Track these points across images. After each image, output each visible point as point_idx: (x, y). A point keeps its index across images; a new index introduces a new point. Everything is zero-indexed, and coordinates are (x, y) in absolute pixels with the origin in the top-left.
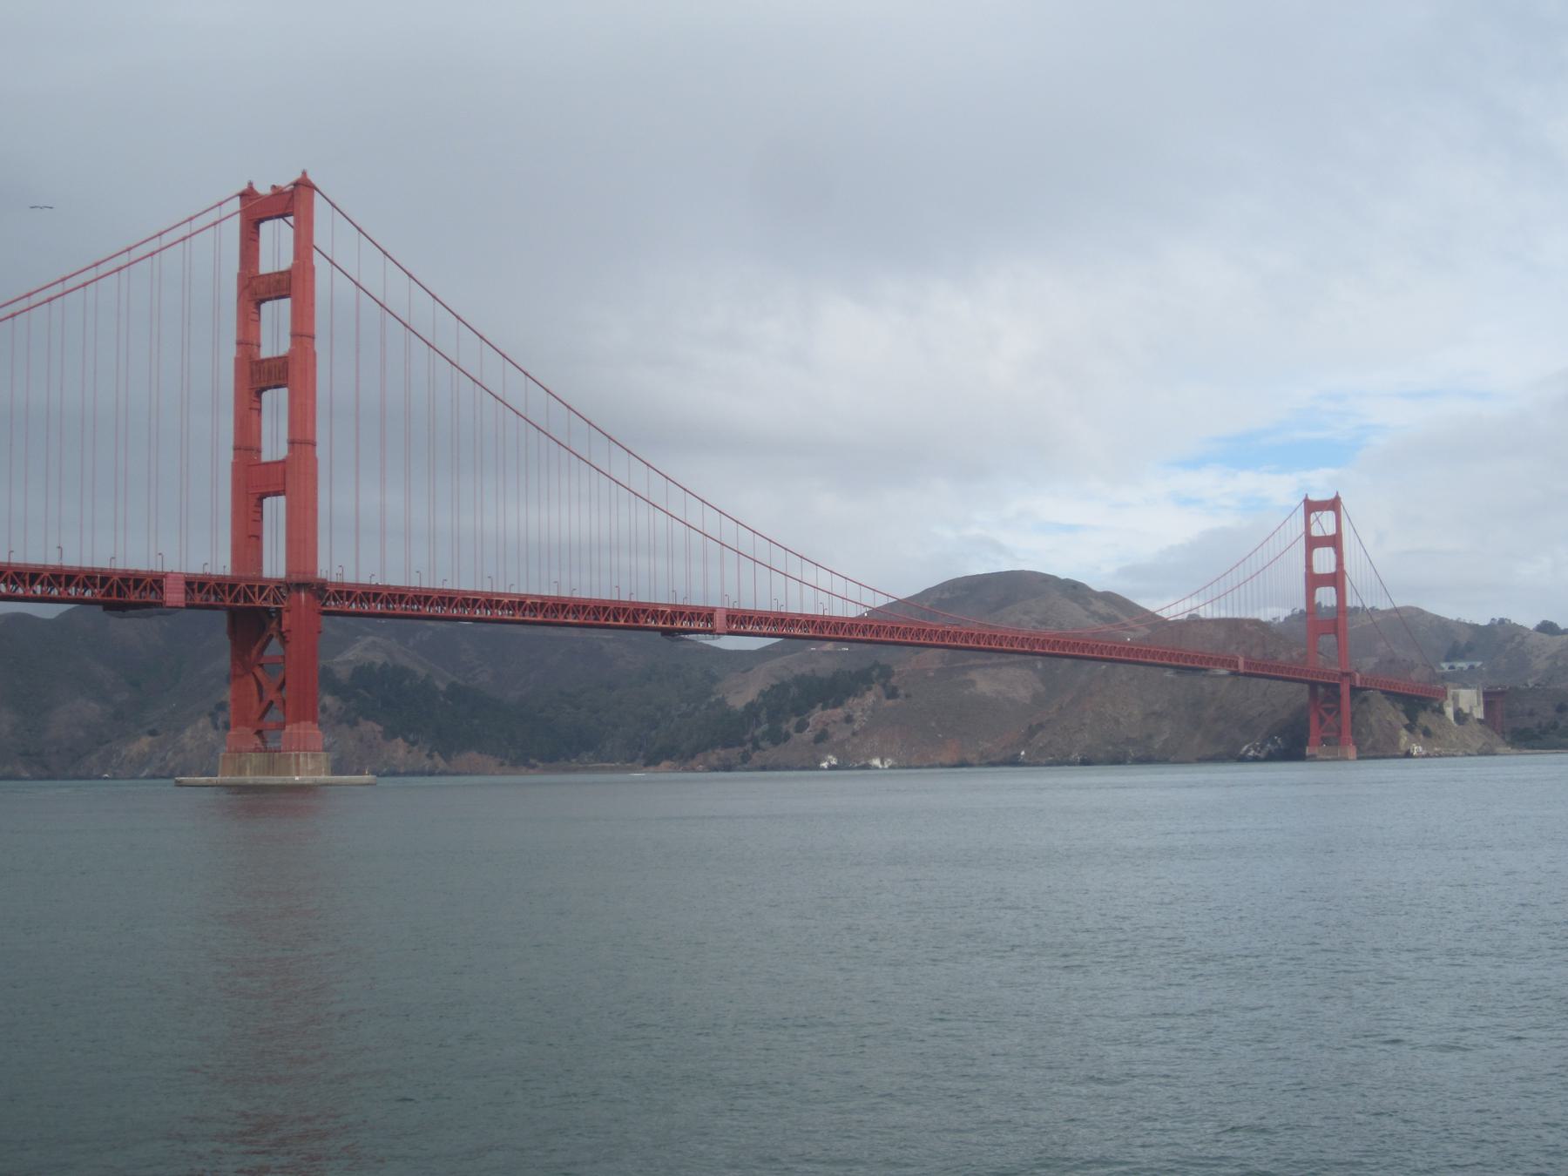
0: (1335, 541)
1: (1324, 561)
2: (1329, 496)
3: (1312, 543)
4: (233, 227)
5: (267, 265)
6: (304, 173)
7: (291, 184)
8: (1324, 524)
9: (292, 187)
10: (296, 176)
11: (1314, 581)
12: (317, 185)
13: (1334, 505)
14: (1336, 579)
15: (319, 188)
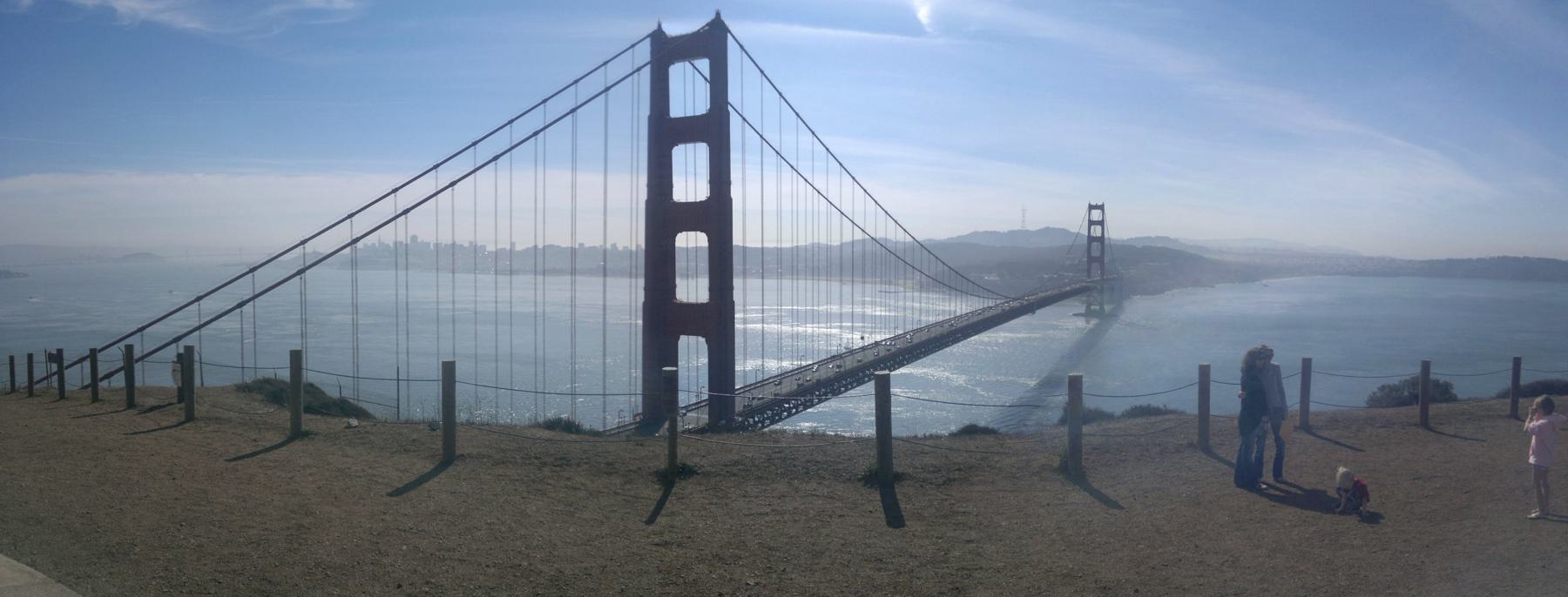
0: (1101, 223)
1: (1097, 231)
2: (1099, 204)
3: (1091, 223)
4: (647, 70)
5: (677, 110)
6: (718, 14)
7: (707, 25)
8: (1096, 215)
9: (707, 28)
10: (711, 17)
11: (1091, 239)
12: (730, 28)
13: (1101, 207)
14: (1101, 239)
15: (732, 32)
